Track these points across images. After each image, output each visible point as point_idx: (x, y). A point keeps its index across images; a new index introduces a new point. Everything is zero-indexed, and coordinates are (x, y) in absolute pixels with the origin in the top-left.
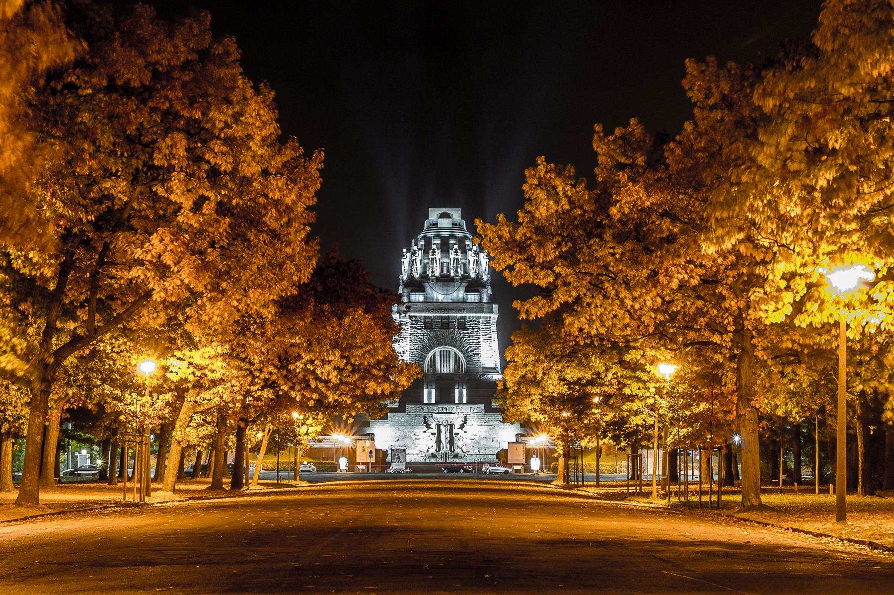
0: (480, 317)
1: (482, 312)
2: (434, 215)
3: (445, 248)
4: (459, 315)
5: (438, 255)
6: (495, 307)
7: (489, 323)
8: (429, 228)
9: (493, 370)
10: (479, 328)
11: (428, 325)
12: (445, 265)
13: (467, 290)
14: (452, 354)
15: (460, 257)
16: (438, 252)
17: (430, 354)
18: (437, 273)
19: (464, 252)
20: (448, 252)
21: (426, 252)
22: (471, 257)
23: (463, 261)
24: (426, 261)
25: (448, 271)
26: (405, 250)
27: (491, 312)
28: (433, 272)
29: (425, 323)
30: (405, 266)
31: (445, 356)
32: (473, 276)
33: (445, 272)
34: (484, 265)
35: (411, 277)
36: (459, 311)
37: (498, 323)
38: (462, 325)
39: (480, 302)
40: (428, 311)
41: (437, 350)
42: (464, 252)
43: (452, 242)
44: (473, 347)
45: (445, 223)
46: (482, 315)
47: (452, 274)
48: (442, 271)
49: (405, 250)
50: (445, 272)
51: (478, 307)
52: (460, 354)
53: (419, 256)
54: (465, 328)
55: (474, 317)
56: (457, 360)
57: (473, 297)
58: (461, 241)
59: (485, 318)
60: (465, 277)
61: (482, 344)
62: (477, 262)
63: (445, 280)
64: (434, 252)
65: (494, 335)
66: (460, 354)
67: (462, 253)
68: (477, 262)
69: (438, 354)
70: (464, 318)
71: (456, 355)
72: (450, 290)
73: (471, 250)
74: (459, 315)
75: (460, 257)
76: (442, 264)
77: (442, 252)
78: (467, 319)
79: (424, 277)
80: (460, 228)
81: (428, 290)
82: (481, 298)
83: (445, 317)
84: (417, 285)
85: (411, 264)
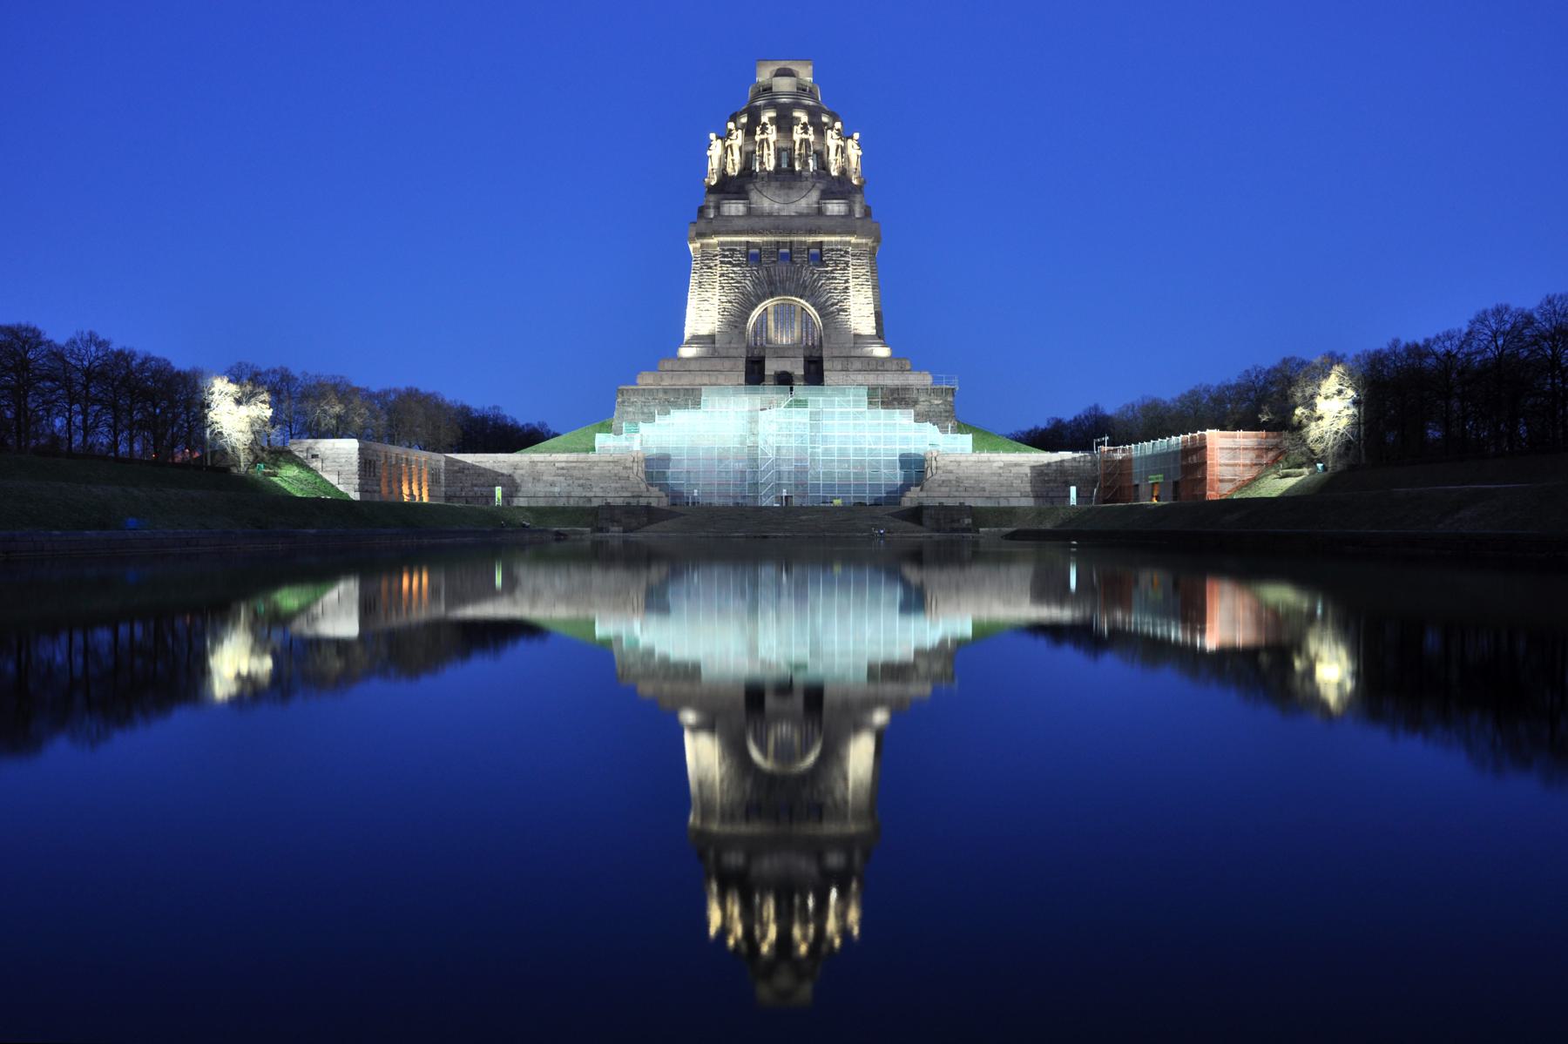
0: (849, 243)
2: (764, 74)
3: (785, 123)
4: (811, 239)
5: (772, 134)
8: (757, 96)
10: (847, 263)
11: (753, 257)
12: (784, 154)
13: (827, 195)
15: (812, 138)
16: (772, 129)
18: (770, 165)
19: (820, 131)
20: (791, 130)
21: (749, 132)
22: (832, 140)
23: (818, 148)
24: (750, 148)
25: (791, 164)
26: (713, 136)
28: (762, 163)
29: (747, 255)
30: (714, 164)
32: (834, 173)
33: (784, 166)
36: (811, 232)
38: (818, 256)
40: (754, 232)
41: (769, 303)
42: (820, 131)
44: (837, 296)
45: (784, 84)
46: (853, 240)
48: (778, 164)
49: (713, 136)
50: (784, 166)
51: (845, 225)
53: (738, 139)
54: (824, 264)
55: (837, 243)
56: (807, 318)
57: (835, 208)
58: (814, 113)
61: (851, 292)
62: (842, 150)
63: (785, 176)
66: (812, 311)
67: (815, 132)
72: (794, 196)
74: (811, 239)
75: (812, 138)
76: (778, 152)
77: (779, 130)
79: (747, 170)
81: (754, 196)
82: (851, 212)
84: (730, 187)
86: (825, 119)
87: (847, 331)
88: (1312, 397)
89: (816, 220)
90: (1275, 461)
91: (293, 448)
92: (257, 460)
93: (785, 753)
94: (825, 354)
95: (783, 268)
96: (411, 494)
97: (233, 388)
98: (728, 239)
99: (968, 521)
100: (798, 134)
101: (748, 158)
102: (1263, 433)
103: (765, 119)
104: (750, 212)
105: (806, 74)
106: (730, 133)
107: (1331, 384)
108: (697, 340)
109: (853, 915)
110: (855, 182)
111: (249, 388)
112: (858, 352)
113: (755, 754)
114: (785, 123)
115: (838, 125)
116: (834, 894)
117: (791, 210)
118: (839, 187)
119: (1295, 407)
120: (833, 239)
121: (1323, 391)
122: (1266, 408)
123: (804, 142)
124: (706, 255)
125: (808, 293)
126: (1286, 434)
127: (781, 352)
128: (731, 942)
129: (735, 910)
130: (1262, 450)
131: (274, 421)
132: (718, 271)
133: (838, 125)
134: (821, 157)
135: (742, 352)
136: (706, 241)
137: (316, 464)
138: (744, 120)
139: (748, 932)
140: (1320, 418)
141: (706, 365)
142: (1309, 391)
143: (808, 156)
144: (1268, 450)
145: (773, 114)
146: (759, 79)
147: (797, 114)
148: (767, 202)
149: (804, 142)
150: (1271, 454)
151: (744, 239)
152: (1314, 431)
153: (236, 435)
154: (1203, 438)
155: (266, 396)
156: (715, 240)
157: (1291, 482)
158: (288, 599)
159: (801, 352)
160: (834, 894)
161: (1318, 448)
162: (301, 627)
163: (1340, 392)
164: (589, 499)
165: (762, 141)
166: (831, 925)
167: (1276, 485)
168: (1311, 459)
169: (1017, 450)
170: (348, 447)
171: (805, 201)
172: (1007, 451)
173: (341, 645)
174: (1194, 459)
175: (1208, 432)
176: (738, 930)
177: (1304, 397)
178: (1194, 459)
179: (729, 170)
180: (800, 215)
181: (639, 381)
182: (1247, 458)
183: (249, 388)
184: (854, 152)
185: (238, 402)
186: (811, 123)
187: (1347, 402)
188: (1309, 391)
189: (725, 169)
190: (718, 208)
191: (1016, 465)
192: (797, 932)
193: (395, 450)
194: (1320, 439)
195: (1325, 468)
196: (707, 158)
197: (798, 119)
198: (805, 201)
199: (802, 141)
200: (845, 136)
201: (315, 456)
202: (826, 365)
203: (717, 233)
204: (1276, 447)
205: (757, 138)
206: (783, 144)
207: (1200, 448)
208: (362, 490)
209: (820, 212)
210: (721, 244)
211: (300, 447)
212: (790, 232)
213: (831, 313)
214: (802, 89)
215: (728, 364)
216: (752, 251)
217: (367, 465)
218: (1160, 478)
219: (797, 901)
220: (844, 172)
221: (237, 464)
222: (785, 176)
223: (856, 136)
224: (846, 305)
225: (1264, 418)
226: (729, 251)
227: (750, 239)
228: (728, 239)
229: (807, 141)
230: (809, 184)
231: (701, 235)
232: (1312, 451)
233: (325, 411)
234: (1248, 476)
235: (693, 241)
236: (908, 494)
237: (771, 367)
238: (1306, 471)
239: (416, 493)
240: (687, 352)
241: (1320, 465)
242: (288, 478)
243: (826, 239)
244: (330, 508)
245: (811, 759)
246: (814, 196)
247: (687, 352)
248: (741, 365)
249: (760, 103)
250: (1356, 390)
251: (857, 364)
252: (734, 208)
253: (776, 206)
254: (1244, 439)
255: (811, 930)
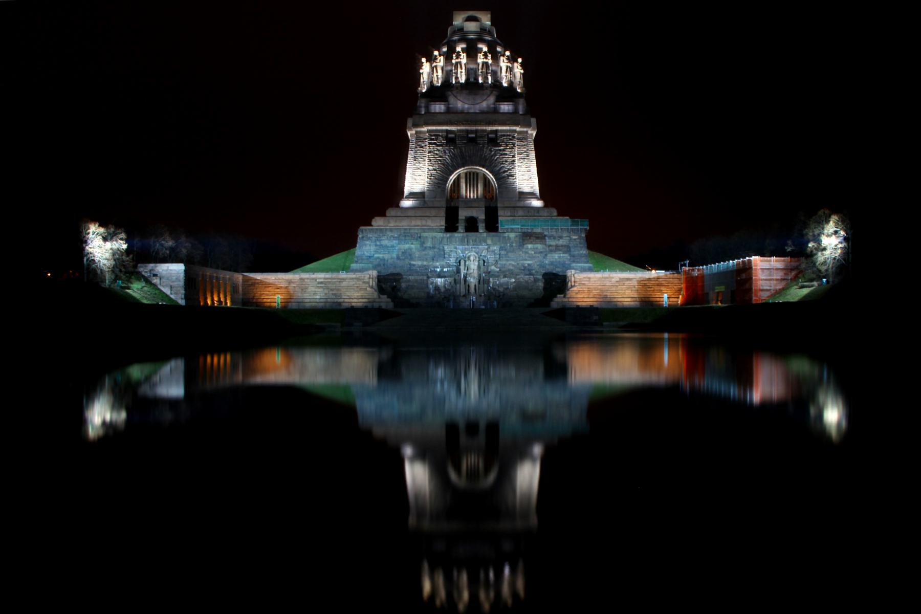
0: (515, 131)
1: (517, 124)
2: (458, 20)
3: (472, 52)
4: (490, 128)
5: (464, 59)
6: (533, 121)
7: (526, 139)
9: (532, 195)
10: (514, 144)
11: (450, 140)
14: (480, 176)
15: (490, 62)
17: (453, 177)
18: (463, 80)
19: (495, 58)
20: (476, 57)
21: (448, 58)
22: (504, 63)
23: (494, 68)
24: (449, 68)
26: (424, 60)
27: (528, 125)
28: (457, 78)
29: (446, 138)
31: (472, 178)
32: (505, 85)
34: (518, 75)
35: (432, 87)
36: (490, 123)
37: (537, 141)
38: (494, 140)
39: (516, 111)
41: (461, 171)
42: (495, 58)
43: (480, 46)
44: (507, 166)
45: (471, 26)
46: (518, 129)
47: (480, 81)
48: (467, 79)
49: (424, 60)
50: (472, 80)
51: (512, 118)
52: (490, 176)
56: (486, 181)
57: (506, 107)
59: (520, 133)
60: (497, 84)
61: (517, 163)
62: (510, 70)
64: (458, 56)
65: (533, 155)
66: (490, 176)
67: (492, 58)
68: (510, 70)
69: (463, 176)
70: (496, 131)
71: (485, 179)
73: (504, 55)
74: (490, 128)
77: (468, 57)
78: (499, 134)
79: (446, 83)
80: (490, 33)
81: (452, 100)
83: (472, 132)
85: (430, 72)
86: (499, 49)
87: (514, 189)
88: (819, 235)
89: (493, 116)
90: (796, 278)
91: (141, 270)
92: (117, 278)
93: (473, 475)
94: (499, 205)
95: (472, 148)
96: (219, 301)
97: (102, 230)
98: (434, 128)
99: (595, 318)
100: (481, 59)
101: (448, 75)
102: (788, 259)
103: (459, 49)
104: (449, 111)
105: (486, 20)
106: (436, 58)
107: (830, 227)
108: (412, 195)
109: (520, 584)
110: (519, 90)
111: (112, 230)
112: (521, 204)
113: (453, 475)
114: (472, 52)
115: (508, 53)
116: (507, 571)
117: (476, 109)
118: (507, 94)
119: (808, 242)
120: (504, 128)
121: (826, 231)
122: (790, 242)
123: (485, 65)
124: (419, 138)
125: (487, 164)
126: (803, 259)
127: (469, 203)
128: (438, 602)
129: (440, 580)
130: (787, 270)
131: (128, 251)
132: (427, 149)
133: (508, 53)
134: (495, 74)
135: (444, 204)
136: (419, 129)
137: (156, 281)
138: (445, 49)
139: (449, 594)
140: (825, 249)
141: (419, 213)
142: (816, 232)
143: (487, 73)
144: (792, 270)
145: (464, 46)
146: (455, 23)
147: (480, 46)
148: (460, 104)
149: (485, 65)
150: (794, 273)
151: (444, 128)
152: (820, 258)
153: (105, 262)
154: (750, 261)
155: (123, 236)
156: (425, 129)
157: (805, 291)
158: (136, 372)
159: (483, 204)
160: (507, 571)
161: (823, 268)
162: (145, 390)
163: (836, 232)
164: (340, 304)
165: (457, 63)
166: (506, 589)
167: (797, 293)
168: (819, 275)
169: (630, 270)
170: (178, 268)
171: (486, 103)
172: (622, 270)
173: (172, 403)
174: (744, 276)
175: (753, 258)
176: (442, 593)
177: (814, 236)
178: (744, 276)
179: (435, 82)
180: (482, 112)
181: (373, 223)
182: (778, 275)
183: (112, 230)
184: (518, 70)
185: (105, 239)
186: (489, 51)
187: (841, 239)
188: (816, 232)
189: (432, 82)
190: (427, 107)
191: (628, 279)
192: (482, 595)
193: (209, 272)
194: (824, 263)
195: (828, 282)
196: (419, 75)
197: (480, 50)
198: (486, 103)
199: (483, 63)
200: (512, 59)
201: (155, 275)
202: (500, 213)
203: (427, 124)
204: (797, 268)
205: (454, 61)
206: (472, 66)
207: (747, 269)
208: (187, 297)
209: (495, 111)
210: (429, 131)
211: (145, 269)
212: (475, 123)
213: (504, 178)
214: (483, 30)
215: (433, 212)
216: (450, 136)
217: (190, 281)
218: (721, 288)
219: (482, 575)
220: (511, 83)
221: (104, 281)
222: (472, 86)
223: (520, 60)
224: (513, 172)
225: (789, 249)
226: (434, 135)
227: (449, 128)
228: (434, 128)
229: (487, 63)
230: (488, 92)
231: (415, 125)
232: (820, 271)
233: (162, 245)
234: (779, 287)
235: (411, 130)
236: (556, 300)
237: (463, 214)
238: (815, 283)
239: (222, 299)
240: (406, 203)
241: (824, 280)
242: (136, 290)
243: (500, 128)
244: (163, 312)
245: (492, 477)
246: (492, 100)
247: (406, 203)
248: (443, 213)
249: (456, 38)
250: (845, 231)
251: (520, 213)
252: (439, 107)
253: (466, 106)
254: (775, 262)
255: (492, 594)
